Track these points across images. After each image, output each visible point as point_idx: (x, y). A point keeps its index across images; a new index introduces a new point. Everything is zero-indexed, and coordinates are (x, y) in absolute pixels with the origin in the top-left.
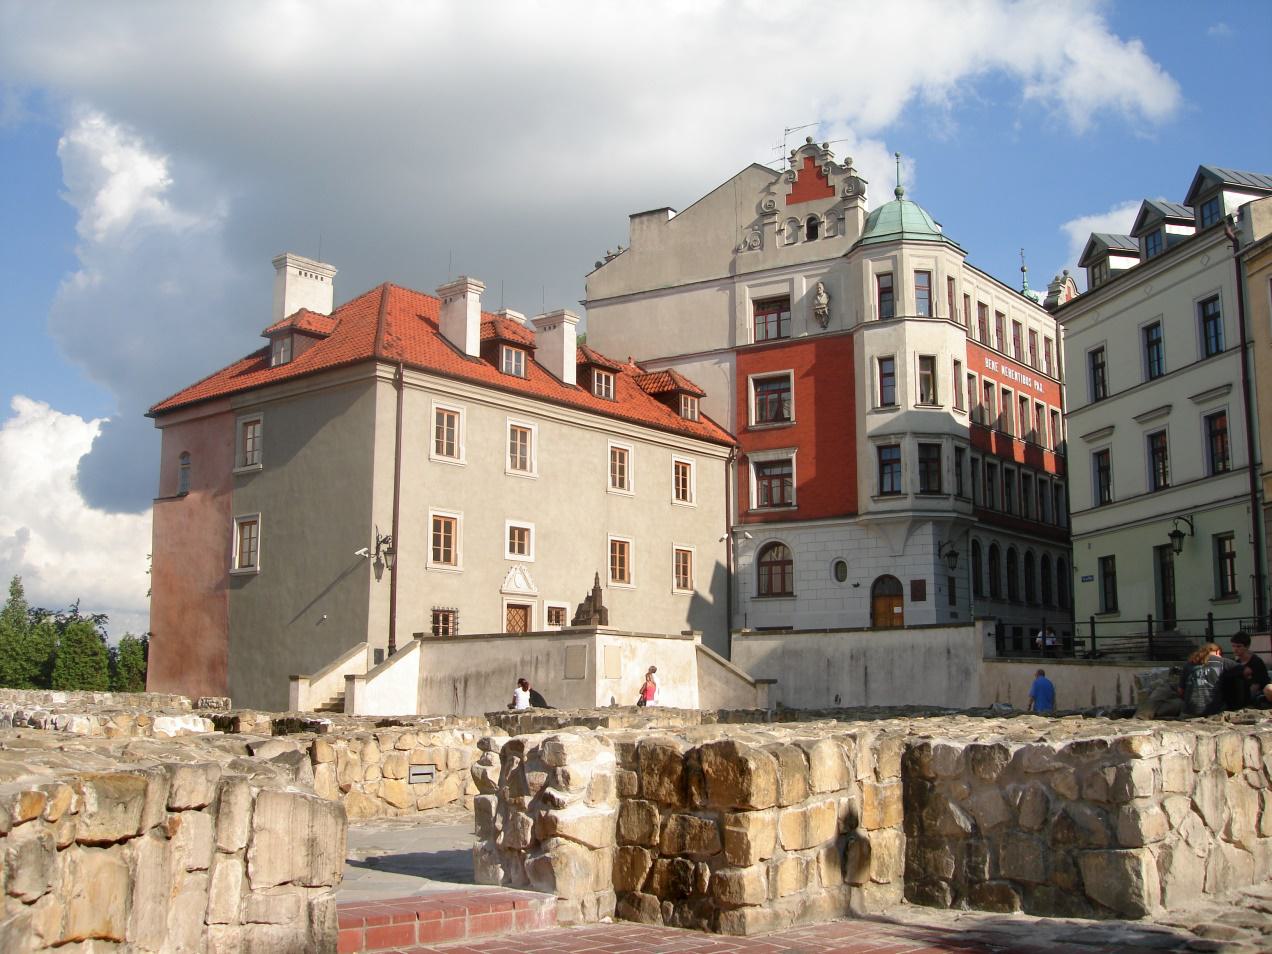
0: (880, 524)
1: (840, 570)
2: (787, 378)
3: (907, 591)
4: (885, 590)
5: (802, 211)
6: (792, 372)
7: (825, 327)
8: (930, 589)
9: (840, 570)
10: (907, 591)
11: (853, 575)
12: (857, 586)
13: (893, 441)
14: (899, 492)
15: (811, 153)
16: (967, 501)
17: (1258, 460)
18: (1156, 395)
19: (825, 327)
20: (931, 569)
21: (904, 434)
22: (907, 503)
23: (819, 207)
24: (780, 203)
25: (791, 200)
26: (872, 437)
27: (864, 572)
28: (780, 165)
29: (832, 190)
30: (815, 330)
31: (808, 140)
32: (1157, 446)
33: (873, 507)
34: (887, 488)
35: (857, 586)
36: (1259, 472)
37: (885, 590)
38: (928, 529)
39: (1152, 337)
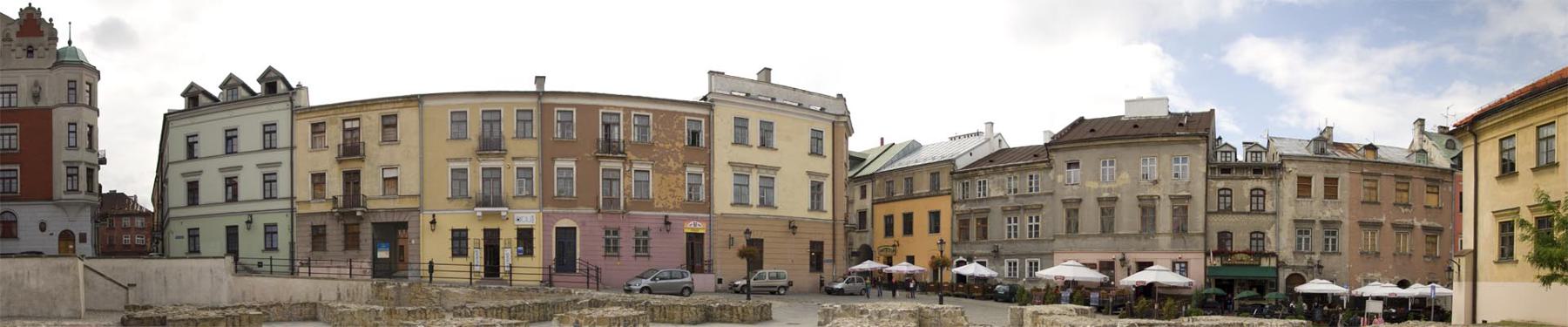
0: (60, 205)
1: (43, 227)
2: (16, 127)
3: (77, 237)
4: (66, 236)
5: (26, 41)
6: (18, 125)
7: (36, 104)
8: (89, 237)
9: (43, 227)
10: (77, 237)
11: (50, 228)
12: (52, 234)
13: (75, 165)
14: (77, 190)
15: (30, 11)
16: (95, 195)
17: (294, 196)
18: (231, 161)
19: (36, 104)
20: (90, 228)
21: (80, 162)
22: (82, 196)
23: (34, 41)
24: (13, 36)
25: (19, 34)
26: (64, 162)
27: (56, 227)
28: (15, 16)
29: (41, 34)
30: (31, 104)
31: (30, 4)
32: (231, 183)
33: (64, 197)
34: (70, 188)
35: (52, 234)
36: (294, 201)
37: (66, 236)
38: (88, 209)
39: (230, 138)
